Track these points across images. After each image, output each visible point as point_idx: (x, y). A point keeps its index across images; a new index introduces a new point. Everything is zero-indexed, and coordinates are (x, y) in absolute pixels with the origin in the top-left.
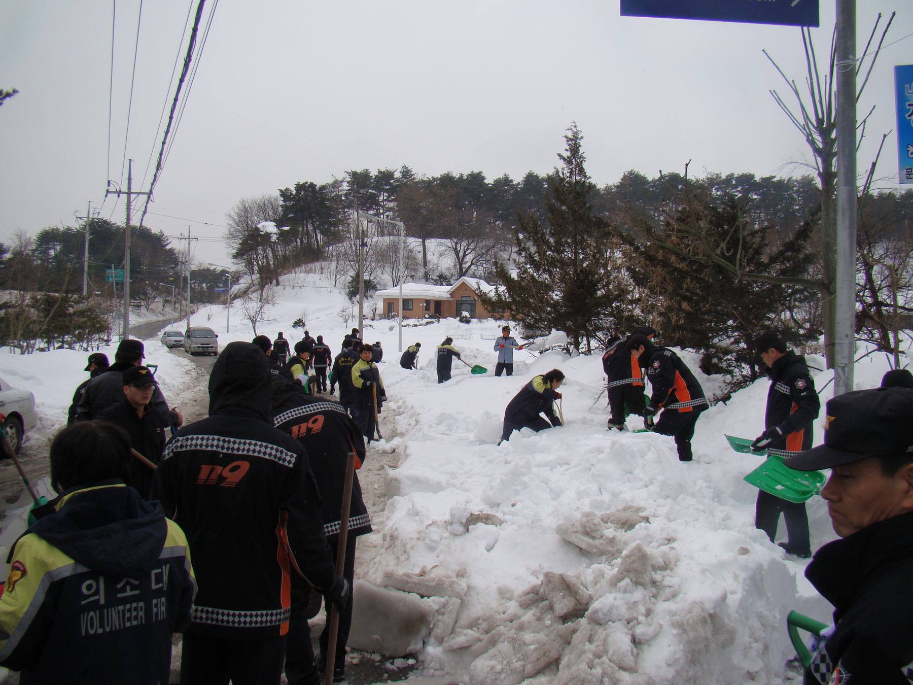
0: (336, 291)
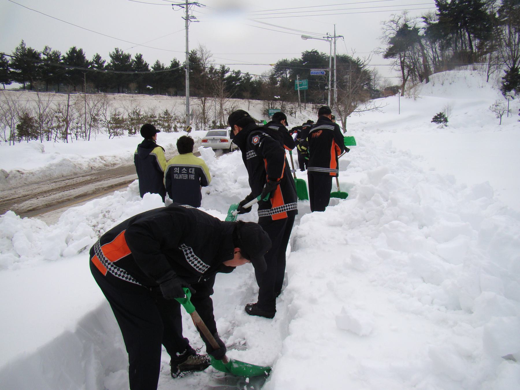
0: (488, 86)
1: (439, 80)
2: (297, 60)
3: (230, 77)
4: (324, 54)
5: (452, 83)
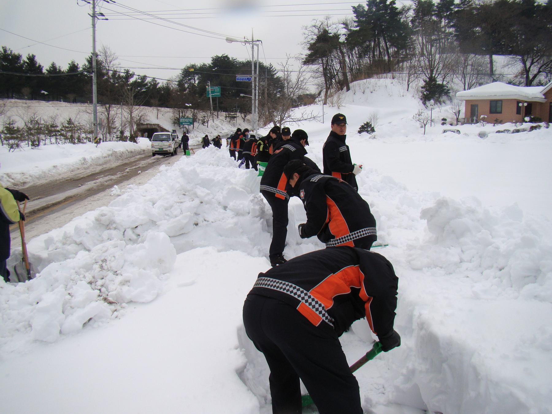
0: (409, 95)
1: (360, 89)
2: (207, 65)
3: (135, 82)
4: (235, 60)
5: (373, 91)
